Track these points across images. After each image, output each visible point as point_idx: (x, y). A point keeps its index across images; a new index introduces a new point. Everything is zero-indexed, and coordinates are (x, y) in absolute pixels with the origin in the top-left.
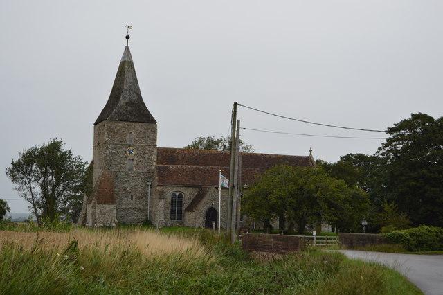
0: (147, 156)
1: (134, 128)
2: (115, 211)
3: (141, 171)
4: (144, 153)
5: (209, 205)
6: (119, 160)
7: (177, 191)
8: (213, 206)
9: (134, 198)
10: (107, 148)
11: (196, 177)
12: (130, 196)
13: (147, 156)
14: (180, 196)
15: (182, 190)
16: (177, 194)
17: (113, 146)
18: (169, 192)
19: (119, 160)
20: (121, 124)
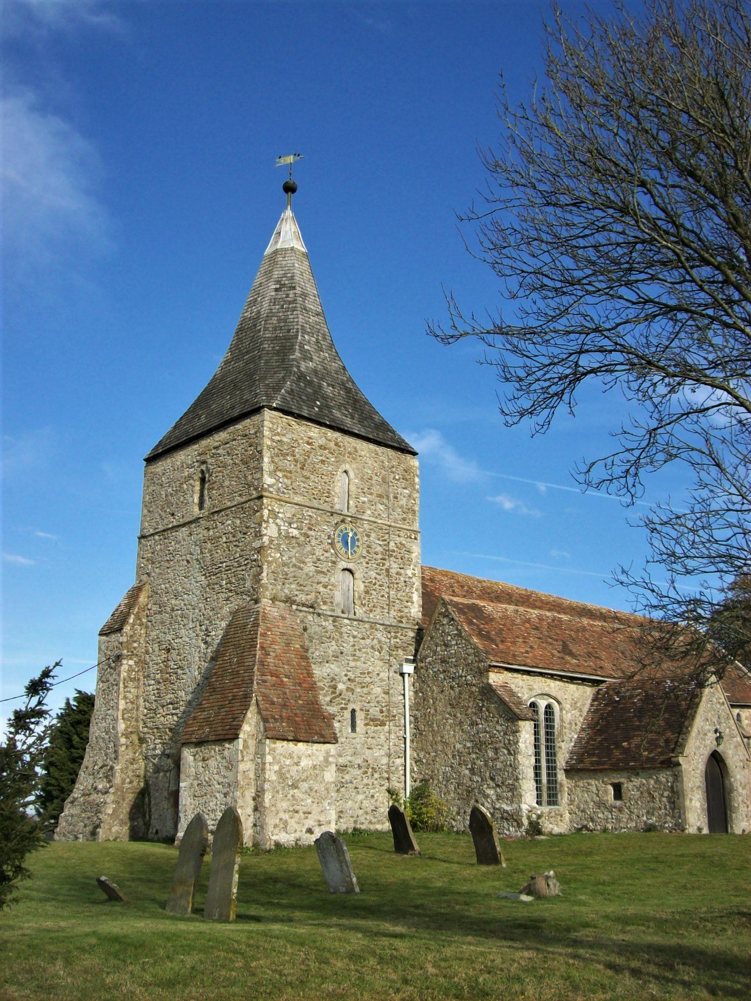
1: (353, 455)
4: (388, 553)
6: (310, 568)
8: (720, 749)
12: (347, 715)
13: (394, 567)
15: (554, 687)
16: (542, 704)
19: (310, 568)
20: (314, 432)
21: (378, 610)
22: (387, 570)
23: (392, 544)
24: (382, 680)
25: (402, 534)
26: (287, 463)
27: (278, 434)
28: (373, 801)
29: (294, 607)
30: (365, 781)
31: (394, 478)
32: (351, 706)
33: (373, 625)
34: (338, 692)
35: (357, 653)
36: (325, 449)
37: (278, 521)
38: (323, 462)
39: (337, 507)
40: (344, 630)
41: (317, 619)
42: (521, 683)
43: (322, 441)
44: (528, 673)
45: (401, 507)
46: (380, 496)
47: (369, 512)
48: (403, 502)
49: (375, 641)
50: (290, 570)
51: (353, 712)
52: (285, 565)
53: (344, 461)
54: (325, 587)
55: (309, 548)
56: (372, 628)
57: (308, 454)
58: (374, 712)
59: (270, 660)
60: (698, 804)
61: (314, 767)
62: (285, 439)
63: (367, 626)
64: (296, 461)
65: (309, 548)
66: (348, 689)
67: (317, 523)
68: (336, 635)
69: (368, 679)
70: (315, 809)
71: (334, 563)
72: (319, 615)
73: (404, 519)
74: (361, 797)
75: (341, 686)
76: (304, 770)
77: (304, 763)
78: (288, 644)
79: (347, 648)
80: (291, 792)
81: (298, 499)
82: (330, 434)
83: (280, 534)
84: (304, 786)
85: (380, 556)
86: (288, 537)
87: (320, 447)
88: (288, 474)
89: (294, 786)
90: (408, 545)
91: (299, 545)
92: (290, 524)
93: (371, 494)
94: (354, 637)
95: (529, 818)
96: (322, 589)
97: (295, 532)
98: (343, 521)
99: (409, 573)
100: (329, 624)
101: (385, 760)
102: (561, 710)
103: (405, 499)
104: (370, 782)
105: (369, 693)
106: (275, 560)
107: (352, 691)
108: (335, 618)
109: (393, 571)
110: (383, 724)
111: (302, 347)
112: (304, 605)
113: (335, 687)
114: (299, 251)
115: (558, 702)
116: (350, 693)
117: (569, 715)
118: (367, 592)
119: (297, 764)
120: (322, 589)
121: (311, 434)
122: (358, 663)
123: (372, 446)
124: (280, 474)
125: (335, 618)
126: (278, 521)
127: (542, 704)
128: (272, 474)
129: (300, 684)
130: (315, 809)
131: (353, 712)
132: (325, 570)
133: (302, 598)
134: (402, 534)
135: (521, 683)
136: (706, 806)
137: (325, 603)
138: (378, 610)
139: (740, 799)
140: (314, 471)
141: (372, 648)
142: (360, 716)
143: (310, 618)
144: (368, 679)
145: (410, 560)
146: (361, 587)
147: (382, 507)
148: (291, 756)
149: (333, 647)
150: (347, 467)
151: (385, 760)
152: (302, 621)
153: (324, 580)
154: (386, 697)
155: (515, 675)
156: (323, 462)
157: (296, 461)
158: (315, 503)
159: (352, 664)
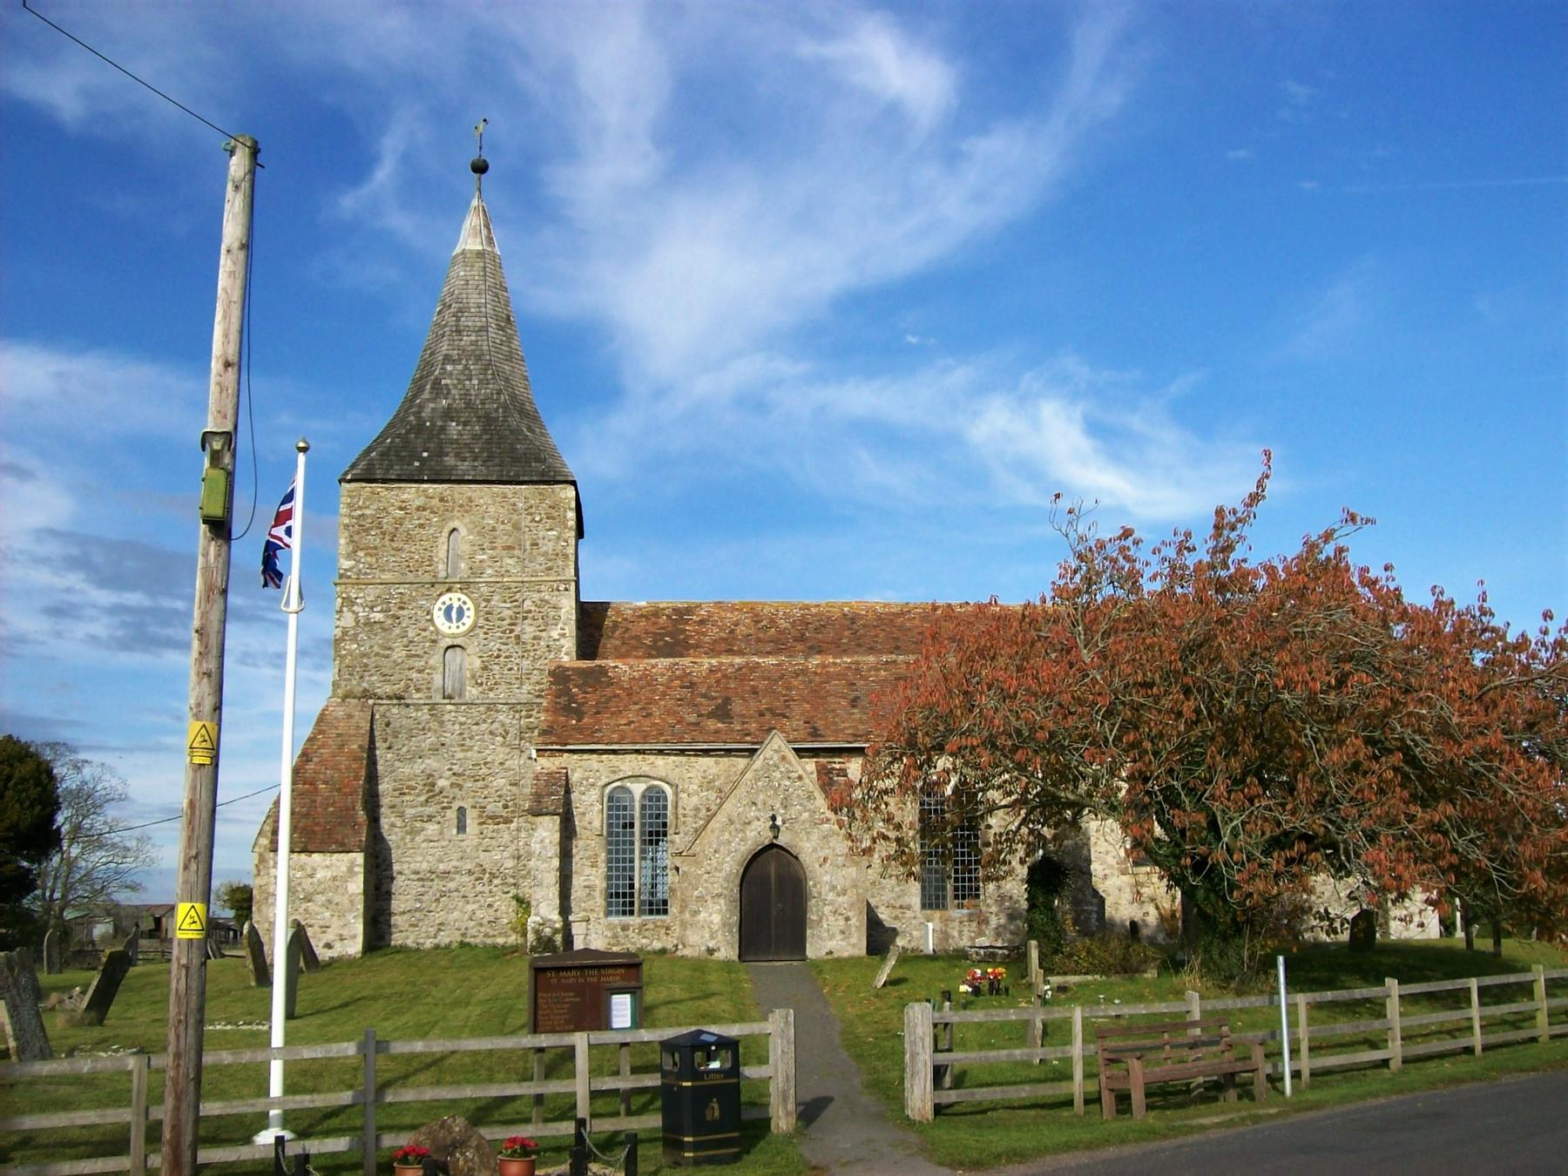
0: (528, 630)
1: (467, 507)
2: (357, 885)
3: (500, 694)
4: (521, 616)
5: (758, 833)
6: (399, 654)
7: (638, 773)
8: (783, 840)
9: (472, 825)
10: (349, 602)
11: (737, 706)
12: (452, 814)
13: (528, 630)
14: (654, 798)
15: (662, 765)
16: (638, 789)
17: (372, 593)
18: (593, 777)
21: (503, 687)
22: (518, 637)
23: (528, 605)
24: (507, 770)
25: (543, 588)
26: (372, 539)
27: (360, 508)
28: (491, 911)
29: (371, 702)
30: (479, 888)
31: (533, 520)
32: (455, 805)
33: (491, 707)
34: (437, 789)
35: (468, 742)
36: (424, 509)
37: (355, 608)
38: (421, 526)
39: (442, 574)
40: (447, 717)
41: (404, 711)
42: (595, 765)
43: (420, 502)
44: (614, 752)
45: (545, 554)
46: (509, 548)
47: (489, 571)
48: (548, 547)
49: (495, 725)
51: (461, 810)
52: (364, 655)
53: (452, 518)
54: (420, 672)
55: (397, 631)
56: (489, 709)
57: (400, 521)
58: (494, 807)
59: (311, 766)
60: (716, 918)
61: (334, 878)
62: (368, 512)
63: (482, 709)
64: (384, 533)
65: (397, 631)
66: (452, 785)
67: (414, 599)
68: (434, 725)
69: (484, 770)
70: (335, 923)
71: (434, 641)
72: (408, 706)
73: (550, 569)
74: (470, 907)
75: (441, 783)
76: (320, 883)
78: (341, 747)
79: (448, 738)
80: (304, 906)
81: (387, 577)
82: (432, 488)
83: (357, 622)
84: (321, 899)
85: (508, 621)
86: (369, 624)
87: (418, 509)
88: (372, 550)
89: (308, 899)
90: (553, 601)
91: (384, 630)
92: (372, 608)
93: (493, 549)
94: (462, 724)
95: (537, 932)
96: (415, 675)
97: (378, 616)
98: (449, 590)
99: (555, 634)
100: (424, 715)
101: (510, 863)
102: (676, 794)
103: (551, 544)
104: (487, 889)
105: (486, 787)
106: (351, 653)
107: (460, 787)
108: (433, 707)
109: (526, 637)
110: (508, 821)
111: (437, 382)
112: (389, 698)
113: (433, 785)
114: (471, 251)
115: (674, 786)
116: (456, 790)
117: (695, 799)
118: (485, 668)
119: (311, 876)
120: (415, 675)
121: (405, 496)
122: (469, 754)
123: (496, 488)
124: (361, 554)
125: (433, 707)
126: (355, 608)
128: (351, 555)
129: (339, 790)
130: (335, 923)
131: (461, 810)
132: (420, 652)
133: (388, 689)
134: (543, 588)
135: (595, 765)
136: (736, 918)
137: (418, 690)
138: (503, 687)
139: (827, 909)
140: (409, 538)
141: (491, 733)
142: (471, 815)
143: (395, 710)
144: (484, 770)
145: (557, 619)
146: (478, 663)
147: (510, 561)
148: (302, 868)
149: (431, 739)
150: (456, 524)
151: (510, 863)
152: (383, 716)
153: (420, 664)
154: (514, 789)
155: (585, 756)
156: (421, 526)
157: (384, 533)
158: (410, 577)
159: (461, 755)
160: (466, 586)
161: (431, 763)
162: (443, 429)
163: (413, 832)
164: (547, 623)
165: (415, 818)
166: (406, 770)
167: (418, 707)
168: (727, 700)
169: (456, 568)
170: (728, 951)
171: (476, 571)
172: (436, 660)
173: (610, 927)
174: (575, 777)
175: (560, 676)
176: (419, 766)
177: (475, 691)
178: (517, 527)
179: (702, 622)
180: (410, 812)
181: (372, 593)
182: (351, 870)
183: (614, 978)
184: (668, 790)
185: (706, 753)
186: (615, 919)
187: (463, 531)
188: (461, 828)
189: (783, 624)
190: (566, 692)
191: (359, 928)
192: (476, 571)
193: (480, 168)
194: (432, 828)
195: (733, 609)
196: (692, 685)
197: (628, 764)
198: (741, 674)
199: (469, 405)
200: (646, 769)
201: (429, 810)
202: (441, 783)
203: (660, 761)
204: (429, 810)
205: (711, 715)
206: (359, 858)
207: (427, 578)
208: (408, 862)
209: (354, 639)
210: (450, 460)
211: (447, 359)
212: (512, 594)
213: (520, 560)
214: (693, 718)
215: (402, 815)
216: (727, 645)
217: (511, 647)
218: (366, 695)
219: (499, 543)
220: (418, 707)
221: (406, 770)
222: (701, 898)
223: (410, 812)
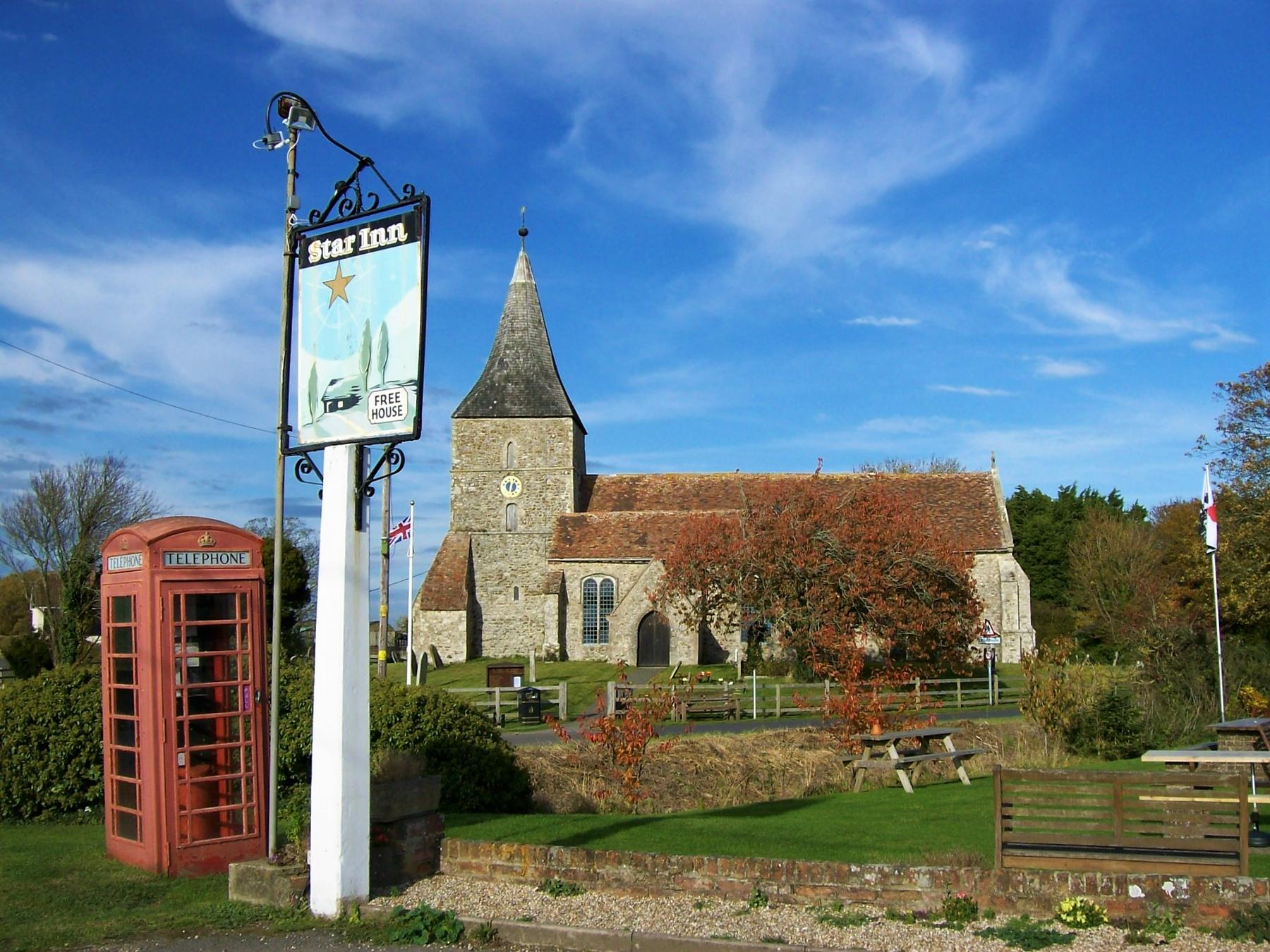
0: (549, 495)
1: (517, 430)
2: (463, 627)
3: (536, 528)
4: (545, 487)
6: (484, 508)
7: (600, 571)
10: (458, 481)
11: (650, 538)
12: (512, 590)
13: (550, 495)
15: (611, 568)
16: (599, 580)
17: (470, 476)
18: (576, 574)
20: (487, 423)
26: (469, 448)
33: (531, 535)
48: (559, 451)
50: (469, 512)
51: (516, 589)
58: (533, 587)
60: (626, 646)
75: (506, 574)
77: (445, 622)
81: (477, 468)
84: (445, 633)
88: (469, 454)
95: (547, 651)
97: (473, 489)
100: (497, 539)
108: (501, 535)
111: (501, 361)
125: (501, 535)
127: (599, 580)
128: (459, 457)
131: (516, 589)
133: (478, 526)
136: (635, 646)
140: (488, 447)
142: (521, 591)
149: (500, 552)
151: (540, 616)
158: (489, 468)
160: (517, 472)
161: (501, 564)
162: (505, 387)
163: (492, 600)
164: (559, 491)
165: (493, 592)
166: (488, 568)
167: (494, 536)
168: (645, 535)
169: (512, 462)
170: (631, 661)
171: (522, 465)
172: (502, 511)
173: (585, 649)
174: (567, 574)
175: (563, 521)
176: (495, 566)
177: (522, 527)
178: (543, 441)
179: (645, 486)
180: (490, 589)
181: (470, 476)
182: (460, 620)
183: (515, 672)
184: (614, 581)
185: (633, 562)
186: (587, 645)
187: (515, 443)
188: (516, 597)
189: (688, 486)
190: (565, 530)
191: (465, 648)
192: (522, 465)
193: (524, 233)
194: (501, 597)
195: (662, 478)
196: (629, 526)
197: (594, 568)
198: (655, 520)
199: (518, 372)
200: (603, 570)
201: (500, 588)
202: (506, 574)
203: (610, 566)
204: (500, 588)
205: (636, 543)
206: (464, 613)
207: (498, 468)
208: (489, 615)
209: (461, 500)
210: (508, 405)
211: (507, 347)
212: (541, 476)
213: (545, 458)
214: (627, 544)
215: (486, 591)
216: (657, 501)
217: (541, 504)
218: (468, 529)
219: (534, 449)
220: (494, 536)
221: (488, 568)
222: (619, 636)
223: (490, 589)
